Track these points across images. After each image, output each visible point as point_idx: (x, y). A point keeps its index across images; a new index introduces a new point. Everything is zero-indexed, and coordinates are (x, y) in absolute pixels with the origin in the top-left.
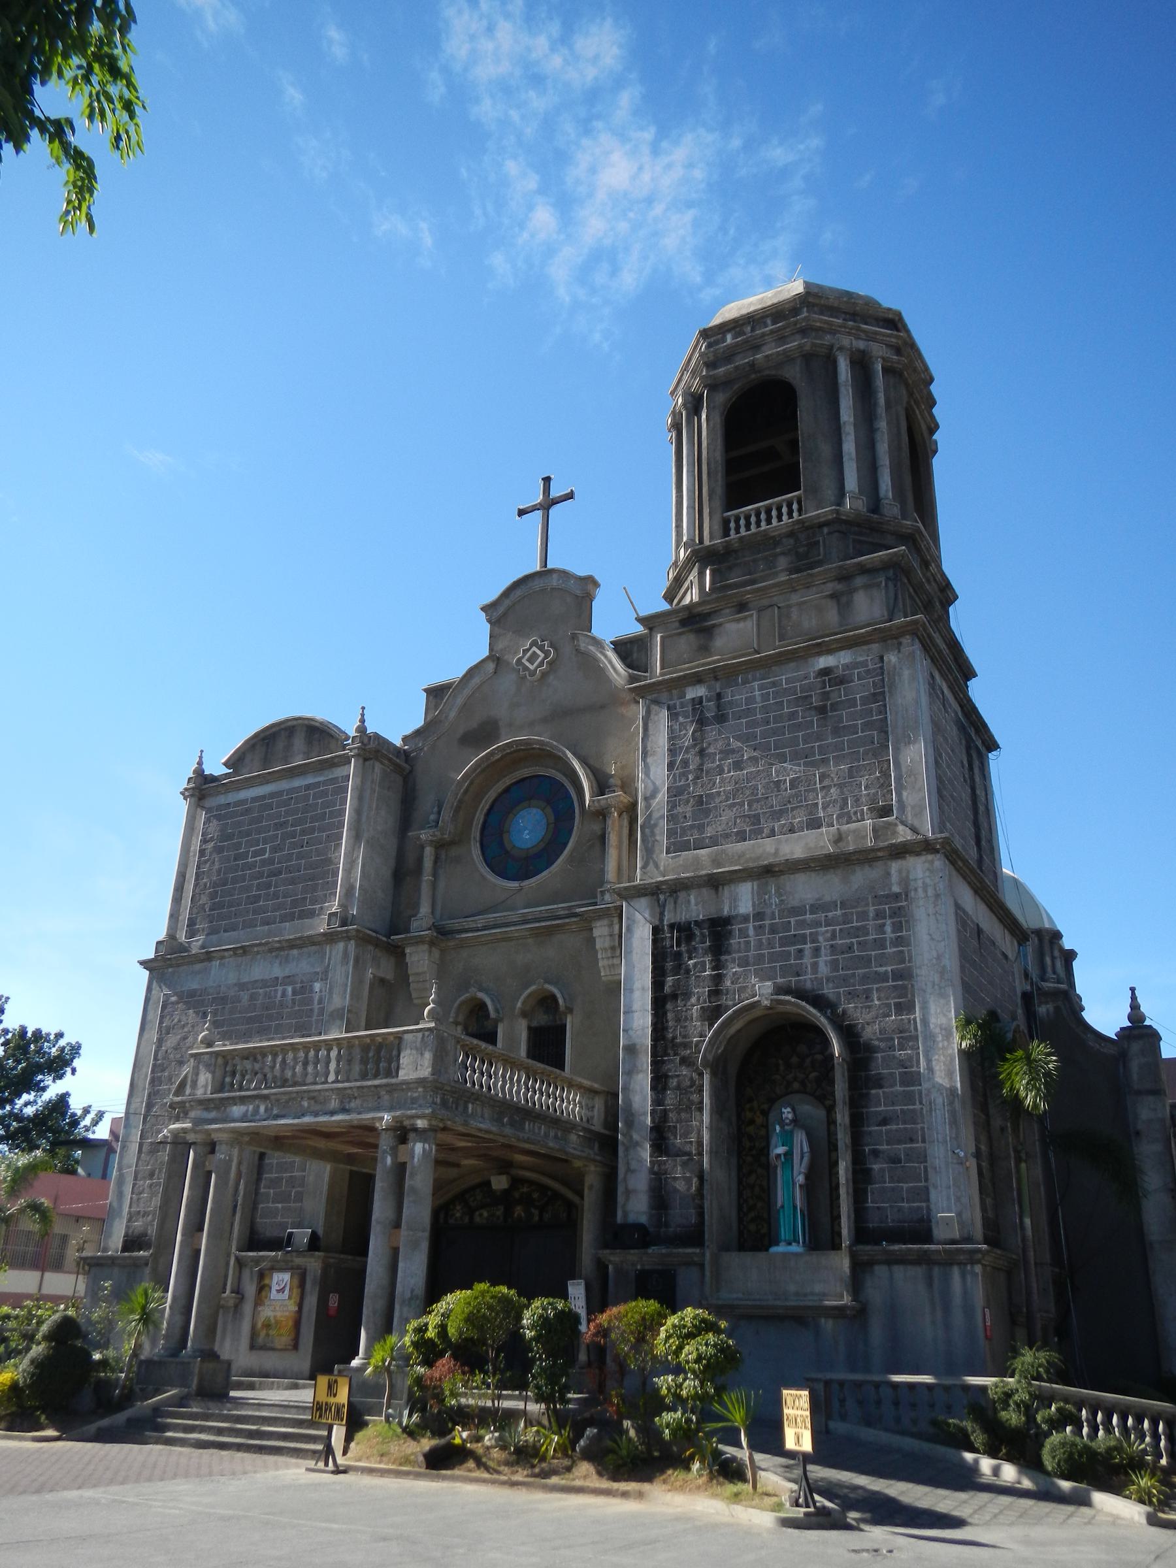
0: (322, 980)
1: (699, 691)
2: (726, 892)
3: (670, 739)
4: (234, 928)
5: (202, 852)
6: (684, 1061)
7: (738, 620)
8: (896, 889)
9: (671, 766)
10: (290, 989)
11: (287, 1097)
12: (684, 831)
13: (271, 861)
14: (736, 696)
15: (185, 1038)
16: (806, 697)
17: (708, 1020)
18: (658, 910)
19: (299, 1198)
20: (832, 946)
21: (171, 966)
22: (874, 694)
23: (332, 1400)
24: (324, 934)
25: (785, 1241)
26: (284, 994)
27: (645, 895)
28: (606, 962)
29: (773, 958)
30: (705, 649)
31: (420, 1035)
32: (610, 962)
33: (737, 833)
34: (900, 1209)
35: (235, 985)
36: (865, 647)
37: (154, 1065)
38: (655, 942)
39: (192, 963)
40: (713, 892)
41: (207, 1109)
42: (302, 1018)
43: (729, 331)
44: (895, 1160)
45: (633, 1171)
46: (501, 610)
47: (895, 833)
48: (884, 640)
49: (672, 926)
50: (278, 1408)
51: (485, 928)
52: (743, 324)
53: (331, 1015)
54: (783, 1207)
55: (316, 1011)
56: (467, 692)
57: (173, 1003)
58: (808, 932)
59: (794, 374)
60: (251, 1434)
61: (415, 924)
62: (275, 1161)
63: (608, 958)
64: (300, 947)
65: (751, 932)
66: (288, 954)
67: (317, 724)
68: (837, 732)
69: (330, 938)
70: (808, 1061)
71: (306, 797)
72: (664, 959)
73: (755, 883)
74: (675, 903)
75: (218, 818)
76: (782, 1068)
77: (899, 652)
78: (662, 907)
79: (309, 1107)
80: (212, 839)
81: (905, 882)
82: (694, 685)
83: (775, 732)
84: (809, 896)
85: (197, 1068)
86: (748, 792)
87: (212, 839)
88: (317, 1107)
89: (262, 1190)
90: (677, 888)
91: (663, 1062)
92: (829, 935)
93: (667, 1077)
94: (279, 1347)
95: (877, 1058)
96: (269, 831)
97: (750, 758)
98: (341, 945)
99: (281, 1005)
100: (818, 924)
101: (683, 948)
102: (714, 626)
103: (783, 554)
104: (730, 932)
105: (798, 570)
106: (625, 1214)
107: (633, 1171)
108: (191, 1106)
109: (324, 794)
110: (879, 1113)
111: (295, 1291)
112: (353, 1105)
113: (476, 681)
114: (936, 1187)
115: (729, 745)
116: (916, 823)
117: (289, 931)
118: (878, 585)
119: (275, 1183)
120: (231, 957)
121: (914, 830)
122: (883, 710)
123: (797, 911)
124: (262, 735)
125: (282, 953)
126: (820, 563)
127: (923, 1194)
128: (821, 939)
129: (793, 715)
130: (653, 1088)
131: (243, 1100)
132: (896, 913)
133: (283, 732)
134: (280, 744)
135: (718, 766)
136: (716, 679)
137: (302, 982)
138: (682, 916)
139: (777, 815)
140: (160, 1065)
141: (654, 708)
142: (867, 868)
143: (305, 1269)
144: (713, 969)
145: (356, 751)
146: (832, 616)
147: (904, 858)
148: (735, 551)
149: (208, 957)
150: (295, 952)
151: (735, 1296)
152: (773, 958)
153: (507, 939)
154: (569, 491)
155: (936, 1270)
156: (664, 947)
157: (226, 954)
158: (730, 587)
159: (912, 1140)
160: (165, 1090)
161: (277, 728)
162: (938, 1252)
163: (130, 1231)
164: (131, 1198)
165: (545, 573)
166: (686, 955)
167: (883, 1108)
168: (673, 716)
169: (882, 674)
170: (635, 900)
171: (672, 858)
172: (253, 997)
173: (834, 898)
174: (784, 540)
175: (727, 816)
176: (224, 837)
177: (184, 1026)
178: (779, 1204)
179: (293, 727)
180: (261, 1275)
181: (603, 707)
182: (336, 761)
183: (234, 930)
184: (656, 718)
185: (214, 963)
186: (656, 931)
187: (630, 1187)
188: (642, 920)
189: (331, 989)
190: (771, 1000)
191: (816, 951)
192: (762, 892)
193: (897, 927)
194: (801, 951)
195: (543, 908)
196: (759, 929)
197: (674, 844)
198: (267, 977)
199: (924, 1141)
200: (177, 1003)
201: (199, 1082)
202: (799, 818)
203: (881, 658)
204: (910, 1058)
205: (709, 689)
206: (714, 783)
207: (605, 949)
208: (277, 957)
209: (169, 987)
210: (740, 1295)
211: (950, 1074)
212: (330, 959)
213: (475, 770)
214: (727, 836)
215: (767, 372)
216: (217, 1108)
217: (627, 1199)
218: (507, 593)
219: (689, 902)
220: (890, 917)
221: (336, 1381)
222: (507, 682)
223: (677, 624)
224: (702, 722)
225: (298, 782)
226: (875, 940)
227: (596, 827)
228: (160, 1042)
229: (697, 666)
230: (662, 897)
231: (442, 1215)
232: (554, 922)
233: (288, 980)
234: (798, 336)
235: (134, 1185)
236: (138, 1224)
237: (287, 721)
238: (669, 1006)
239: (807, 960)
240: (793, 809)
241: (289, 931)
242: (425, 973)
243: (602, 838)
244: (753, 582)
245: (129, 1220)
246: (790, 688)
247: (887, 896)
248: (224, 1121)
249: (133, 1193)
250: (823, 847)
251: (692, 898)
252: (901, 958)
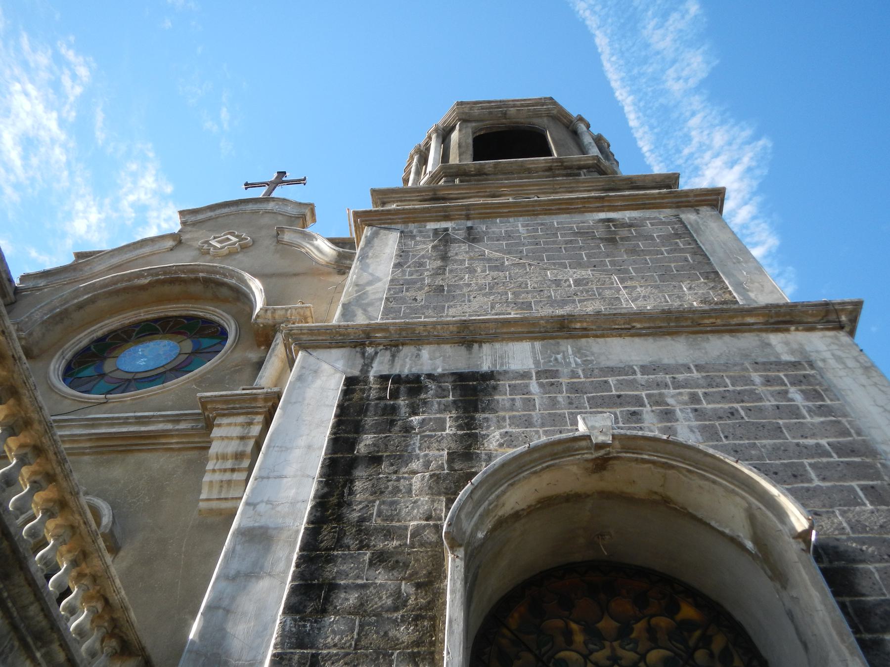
6: (380, 559)
17: (446, 494)
27: (339, 345)
32: (227, 476)
49: (384, 378)
63: (225, 470)
70: (640, 626)
72: (363, 410)
73: (538, 345)
76: (579, 638)
77: (698, 213)
91: (330, 560)
92: (686, 398)
93: (333, 587)
95: (868, 573)
113: (147, 250)
130: (290, 609)
135: (467, 268)
144: (460, 427)
147: (787, 330)
166: (404, 410)
184: (384, 237)
238: (360, 472)
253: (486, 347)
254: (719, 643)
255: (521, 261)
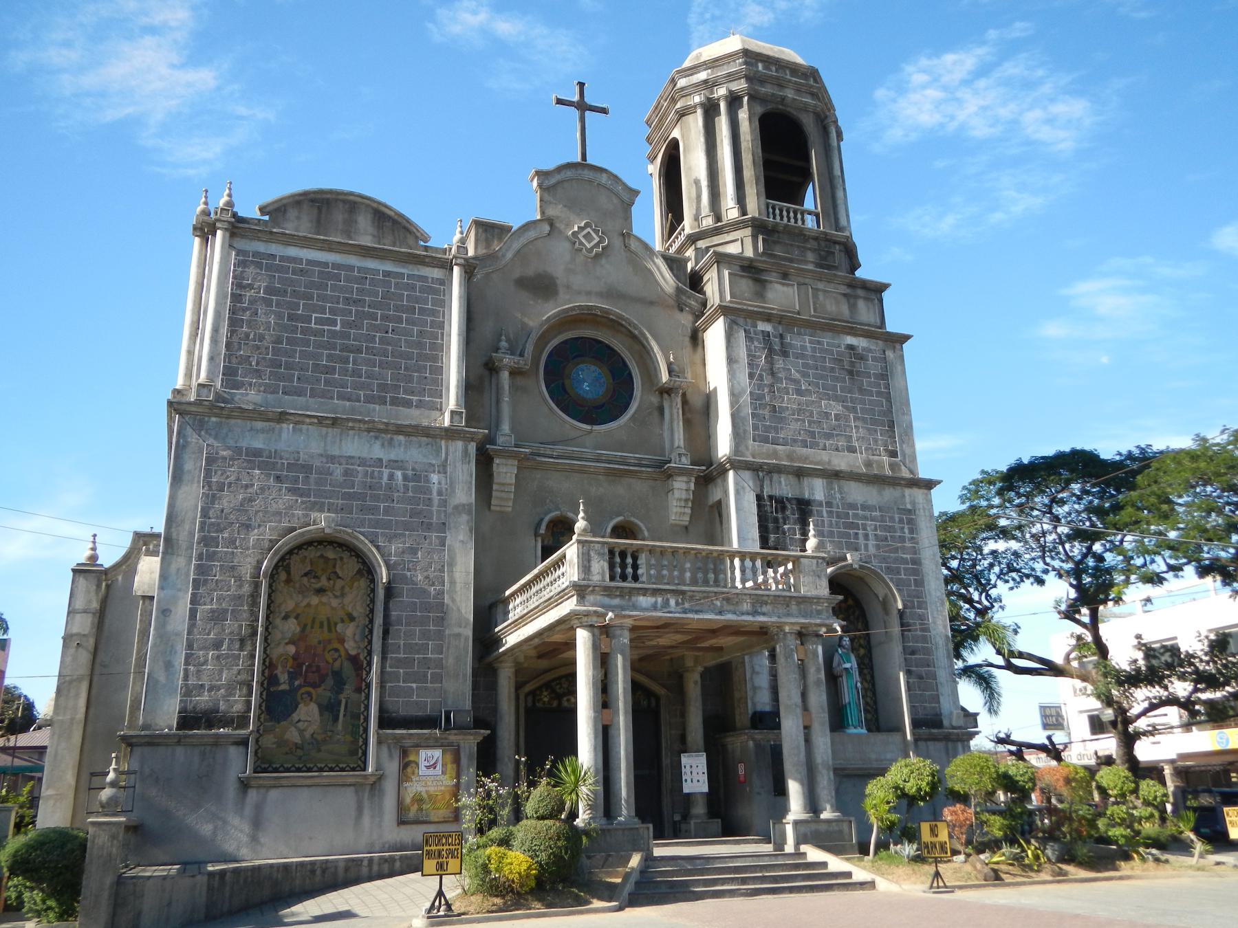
0: (439, 472)
1: (767, 327)
2: (806, 481)
3: (749, 355)
4: (300, 393)
5: (236, 298)
7: (783, 284)
8: (909, 507)
9: (751, 376)
10: (399, 474)
11: (701, 595)
12: (767, 429)
13: (344, 335)
14: (793, 340)
15: (251, 500)
16: (840, 360)
18: (758, 483)
19: (438, 678)
20: (875, 535)
21: (216, 415)
22: (882, 375)
23: (934, 839)
24: (446, 430)
25: (853, 725)
26: (391, 477)
27: (749, 469)
28: (679, 510)
29: (841, 535)
30: (760, 295)
31: (814, 561)
32: (683, 510)
33: (802, 441)
34: (925, 707)
35: (322, 455)
36: (874, 341)
37: (203, 524)
38: (759, 506)
39: (251, 419)
40: (796, 479)
41: (608, 596)
42: (418, 505)
43: (762, 61)
44: (921, 677)
45: (758, 673)
46: (553, 181)
47: (900, 469)
48: (886, 340)
49: (771, 497)
50: (751, 859)
51: (558, 457)
52: (772, 63)
53: (456, 507)
54: (850, 703)
55: (436, 502)
56: (523, 240)
57: (224, 458)
58: (860, 522)
59: (809, 123)
60: (775, 879)
61: (501, 440)
62: (402, 642)
63: (681, 507)
64: (407, 434)
65: (825, 514)
66: (392, 439)
67: (392, 213)
68: (862, 391)
69: (450, 434)
71: (388, 284)
74: (771, 481)
75: (259, 265)
78: (762, 481)
79: (722, 606)
80: (251, 287)
81: (913, 503)
82: (763, 321)
83: (822, 377)
84: (859, 498)
85: (589, 555)
86: (808, 414)
87: (251, 287)
88: (731, 608)
89: (388, 669)
90: (775, 470)
92: (873, 527)
94: (437, 820)
96: (338, 303)
97: (806, 390)
98: (460, 444)
99: (389, 488)
100: (865, 518)
101: (780, 516)
102: (766, 281)
103: (810, 249)
104: (811, 511)
105: (821, 266)
106: (754, 704)
107: (758, 673)
108: (593, 591)
109: (413, 288)
110: (910, 646)
111: (449, 766)
112: (764, 609)
113: (532, 234)
114: (942, 695)
115: (791, 374)
116: (912, 467)
117: (380, 413)
118: (872, 300)
119: (399, 663)
120: (311, 424)
121: (911, 472)
122: (887, 386)
123: (853, 506)
124: (312, 195)
125: (383, 435)
126: (836, 268)
127: (936, 699)
128: (868, 528)
129: (832, 370)
131: (655, 592)
132: (910, 522)
133: (341, 205)
134: (339, 216)
136: (780, 323)
137: (413, 469)
138: (777, 492)
139: (828, 436)
140: (213, 524)
141: (735, 327)
142: (891, 489)
143: (458, 746)
145: (462, 261)
146: (845, 310)
148: (778, 232)
149: (282, 417)
150: (401, 438)
151: (839, 762)
152: (841, 535)
153: (582, 471)
154: (604, 106)
155: (950, 745)
156: (766, 511)
157: (308, 420)
158: (775, 255)
159: (928, 666)
160: (226, 553)
161: (334, 196)
162: (958, 734)
163: (190, 707)
164: (186, 671)
165: (583, 165)
166: (781, 521)
167: (911, 644)
168: (749, 338)
169: (886, 363)
170: (741, 471)
171: (758, 445)
172: (347, 473)
173: (874, 503)
174: (811, 240)
175: (795, 426)
176: (270, 290)
177: (247, 486)
178: (847, 701)
179: (355, 203)
180: (404, 752)
181: (652, 303)
182: (427, 260)
183: (300, 396)
185: (285, 425)
186: (759, 498)
187: (756, 684)
188: (748, 489)
189: (452, 483)
190: (860, 565)
191: (866, 537)
192: (829, 487)
193: (912, 531)
194: (857, 534)
195: (620, 454)
196: (830, 513)
197: (759, 435)
198: (364, 455)
199: (934, 667)
200: (232, 459)
201: (592, 569)
202: (842, 443)
203: (884, 351)
204: (924, 614)
205: (774, 328)
206: (784, 400)
207: (680, 500)
208: (376, 438)
209: (216, 438)
210: (842, 762)
211: (945, 627)
212: (447, 454)
213: (555, 317)
214: (795, 441)
215: (788, 109)
216: (621, 596)
217: (755, 693)
218: (561, 169)
219: (780, 482)
220: (907, 524)
221: (936, 826)
222: (561, 249)
223: (738, 268)
224: (771, 351)
225: (371, 264)
226: (900, 536)
227: (655, 399)
228: (210, 499)
229: (756, 306)
230: (761, 474)
231: (530, 699)
232: (622, 467)
233: (395, 464)
234: (809, 96)
235: (188, 657)
236: (203, 700)
237: (351, 194)
239: (861, 541)
240: (837, 435)
241: (380, 413)
242: (511, 484)
243: (661, 410)
244: (791, 260)
245: (188, 692)
246: (829, 350)
247: (904, 510)
248: (635, 608)
249: (187, 663)
250: (858, 467)
251: (782, 479)
252: (915, 551)
253: (805, 478)
254: (857, 613)
255: (810, 388)
